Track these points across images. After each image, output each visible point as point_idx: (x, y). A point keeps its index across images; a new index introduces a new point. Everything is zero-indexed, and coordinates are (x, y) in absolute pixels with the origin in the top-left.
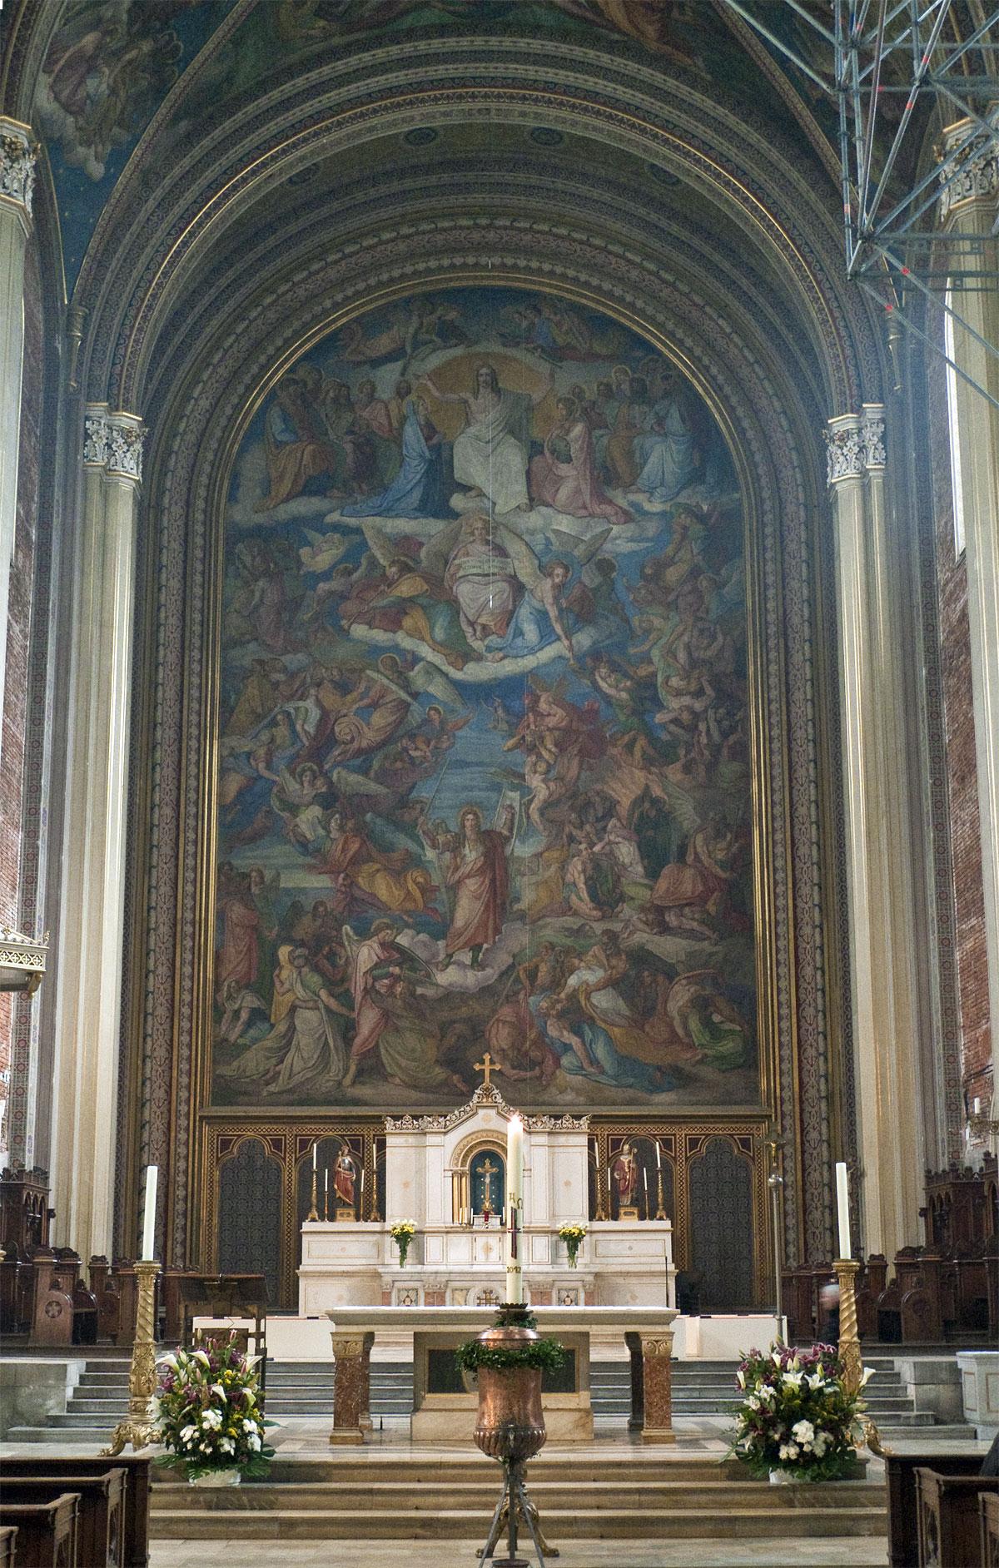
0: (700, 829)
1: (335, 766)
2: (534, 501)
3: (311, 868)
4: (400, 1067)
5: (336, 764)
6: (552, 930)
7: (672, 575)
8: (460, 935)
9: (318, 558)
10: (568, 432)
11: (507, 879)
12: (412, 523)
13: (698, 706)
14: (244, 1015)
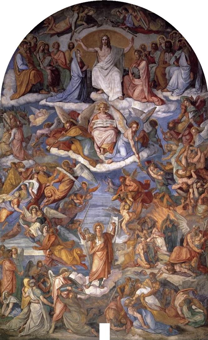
0: (189, 232)
1: (44, 207)
2: (125, 95)
3: (35, 248)
4: (71, 326)
5: (45, 206)
6: (130, 272)
7: (180, 127)
8: (95, 274)
9: (37, 120)
10: (139, 65)
11: (112, 252)
12: (75, 105)
13: (190, 182)
14: (11, 306)
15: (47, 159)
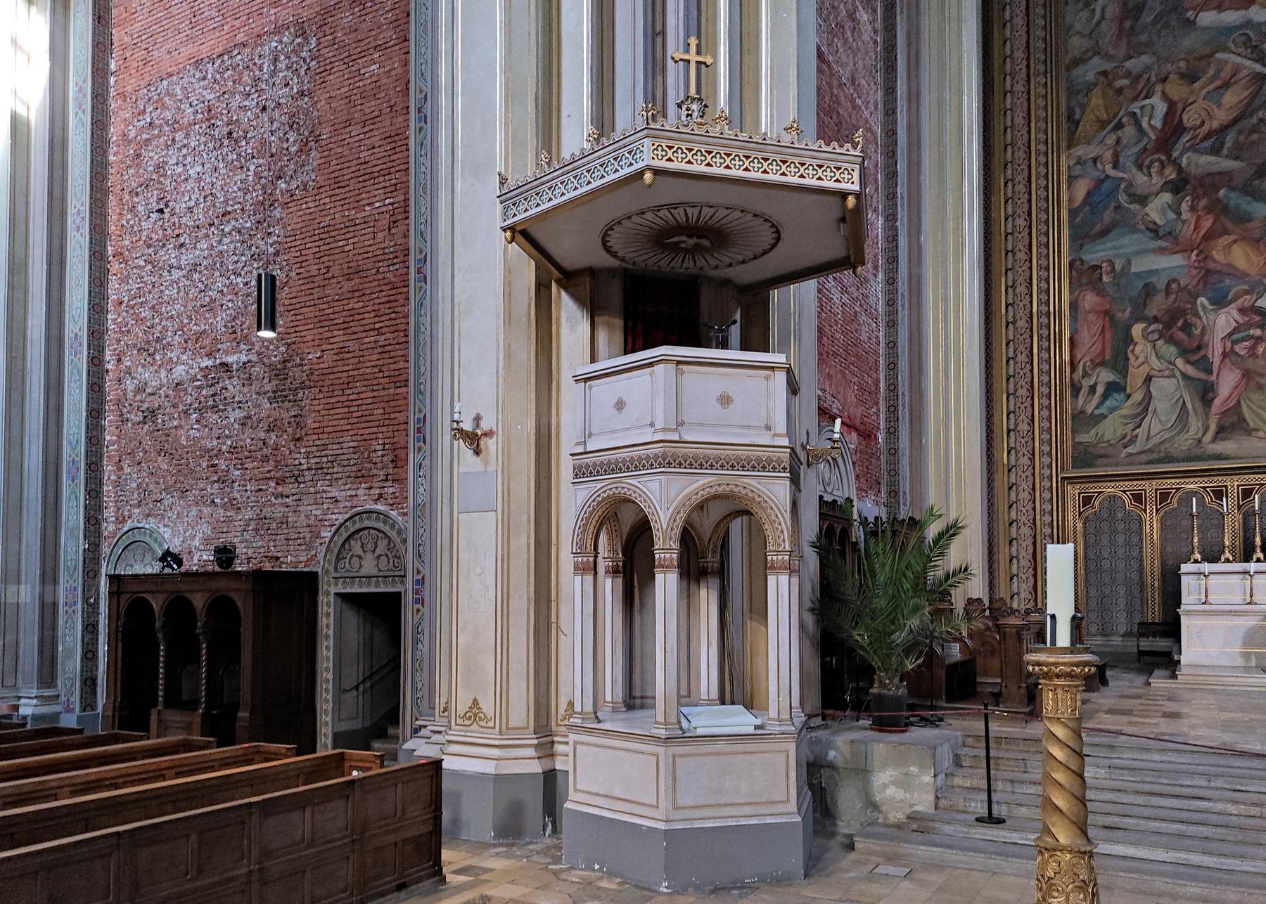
1: (1182, 155)
3: (1162, 251)
5: (1185, 150)
14: (1100, 389)
15: (1189, 42)
